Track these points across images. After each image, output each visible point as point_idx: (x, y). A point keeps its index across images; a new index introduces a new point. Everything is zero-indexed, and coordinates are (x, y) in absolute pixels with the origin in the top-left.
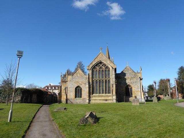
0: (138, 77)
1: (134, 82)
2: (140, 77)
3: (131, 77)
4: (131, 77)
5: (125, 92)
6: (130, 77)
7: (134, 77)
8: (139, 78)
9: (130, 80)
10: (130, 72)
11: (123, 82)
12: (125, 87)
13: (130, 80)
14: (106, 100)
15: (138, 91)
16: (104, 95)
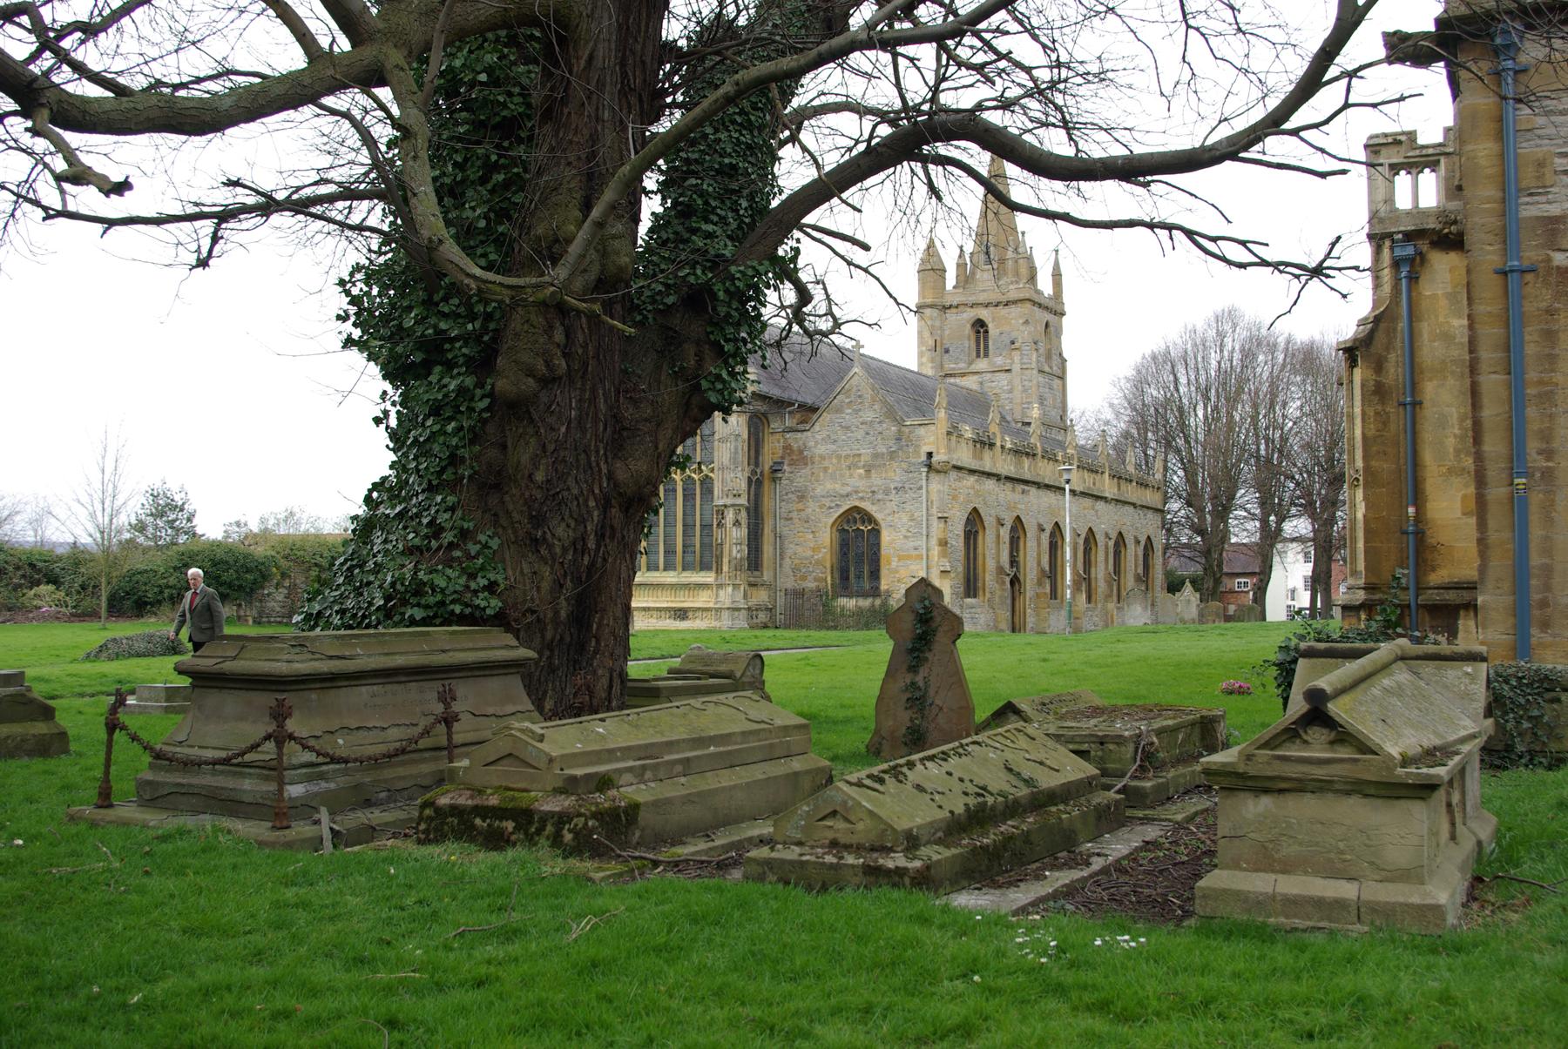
0: (917, 452)
1: (887, 492)
2: (930, 455)
3: (876, 456)
4: (876, 456)
5: (828, 565)
6: (866, 452)
7: (892, 455)
8: (924, 458)
9: (868, 471)
10: (869, 415)
11: (819, 491)
12: (832, 520)
13: (868, 471)
14: (681, 614)
15: (909, 557)
16: (670, 577)
